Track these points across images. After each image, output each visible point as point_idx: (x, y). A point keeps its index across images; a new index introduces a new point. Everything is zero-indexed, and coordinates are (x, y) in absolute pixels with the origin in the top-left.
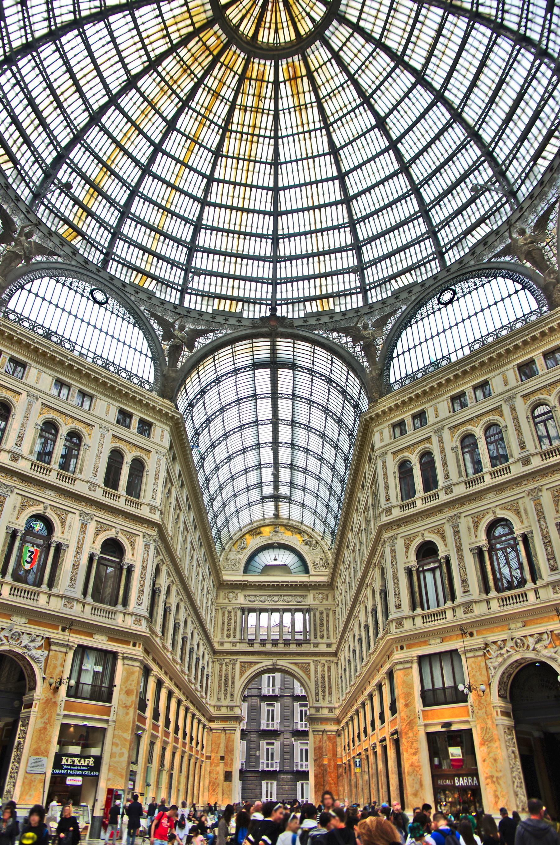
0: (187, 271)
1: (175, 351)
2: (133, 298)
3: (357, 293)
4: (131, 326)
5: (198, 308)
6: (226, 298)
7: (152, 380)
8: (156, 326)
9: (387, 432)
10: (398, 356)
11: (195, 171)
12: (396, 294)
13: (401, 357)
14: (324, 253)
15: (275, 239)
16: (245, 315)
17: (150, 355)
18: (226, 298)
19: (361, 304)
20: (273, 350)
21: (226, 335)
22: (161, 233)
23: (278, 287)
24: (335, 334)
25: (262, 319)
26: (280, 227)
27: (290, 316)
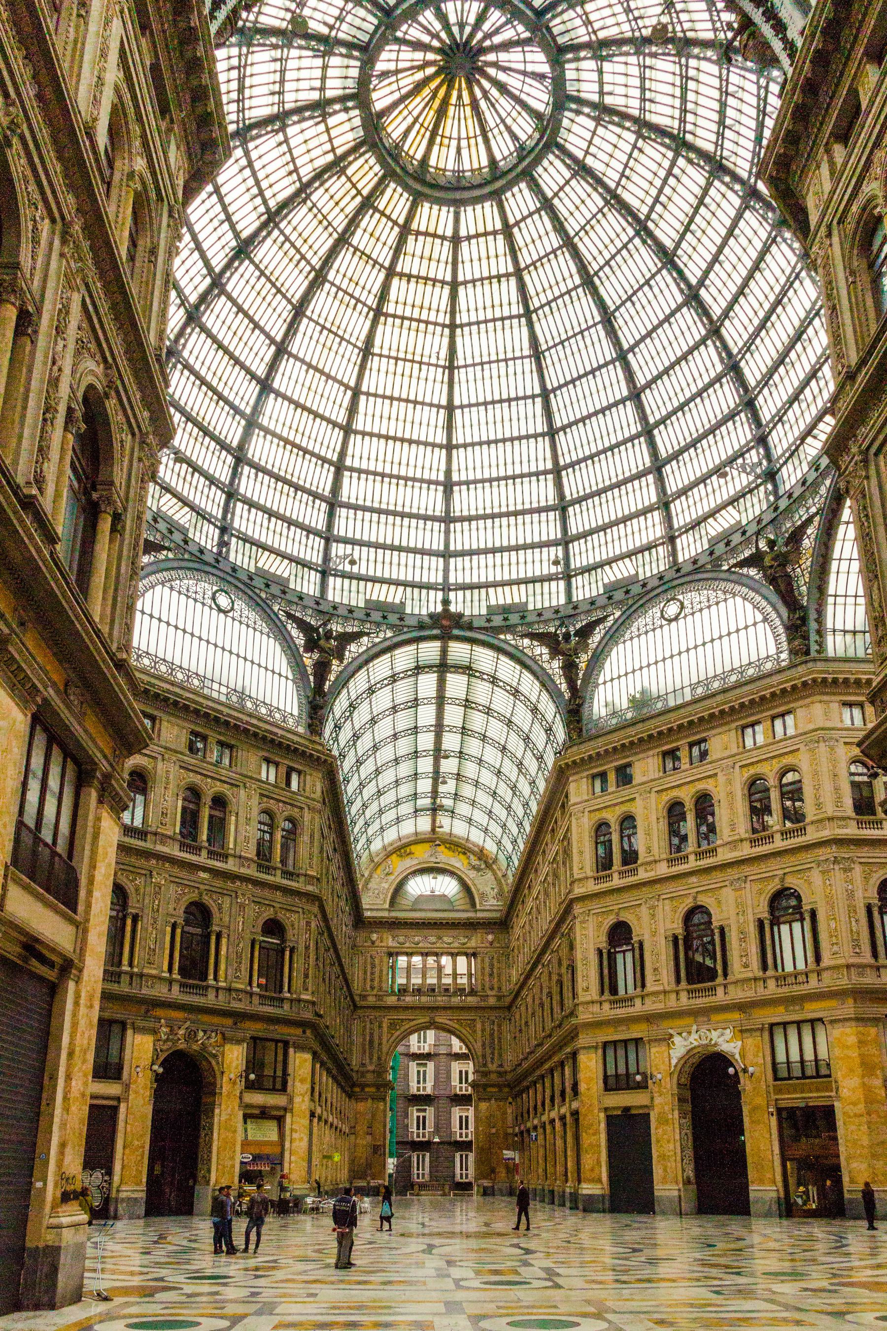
0: (328, 540)
1: (322, 669)
2: (263, 595)
3: (558, 579)
4: (265, 637)
5: (346, 601)
6: (382, 581)
7: (296, 712)
8: (295, 632)
9: (584, 784)
10: (605, 683)
11: (335, 379)
12: (610, 590)
13: (609, 684)
14: (516, 514)
15: (448, 486)
16: (408, 610)
17: (290, 676)
18: (382, 581)
19: (562, 601)
20: (444, 652)
21: (385, 639)
22: (290, 483)
23: (452, 560)
24: (526, 642)
25: (431, 616)
26: (455, 467)
27: (467, 613)
